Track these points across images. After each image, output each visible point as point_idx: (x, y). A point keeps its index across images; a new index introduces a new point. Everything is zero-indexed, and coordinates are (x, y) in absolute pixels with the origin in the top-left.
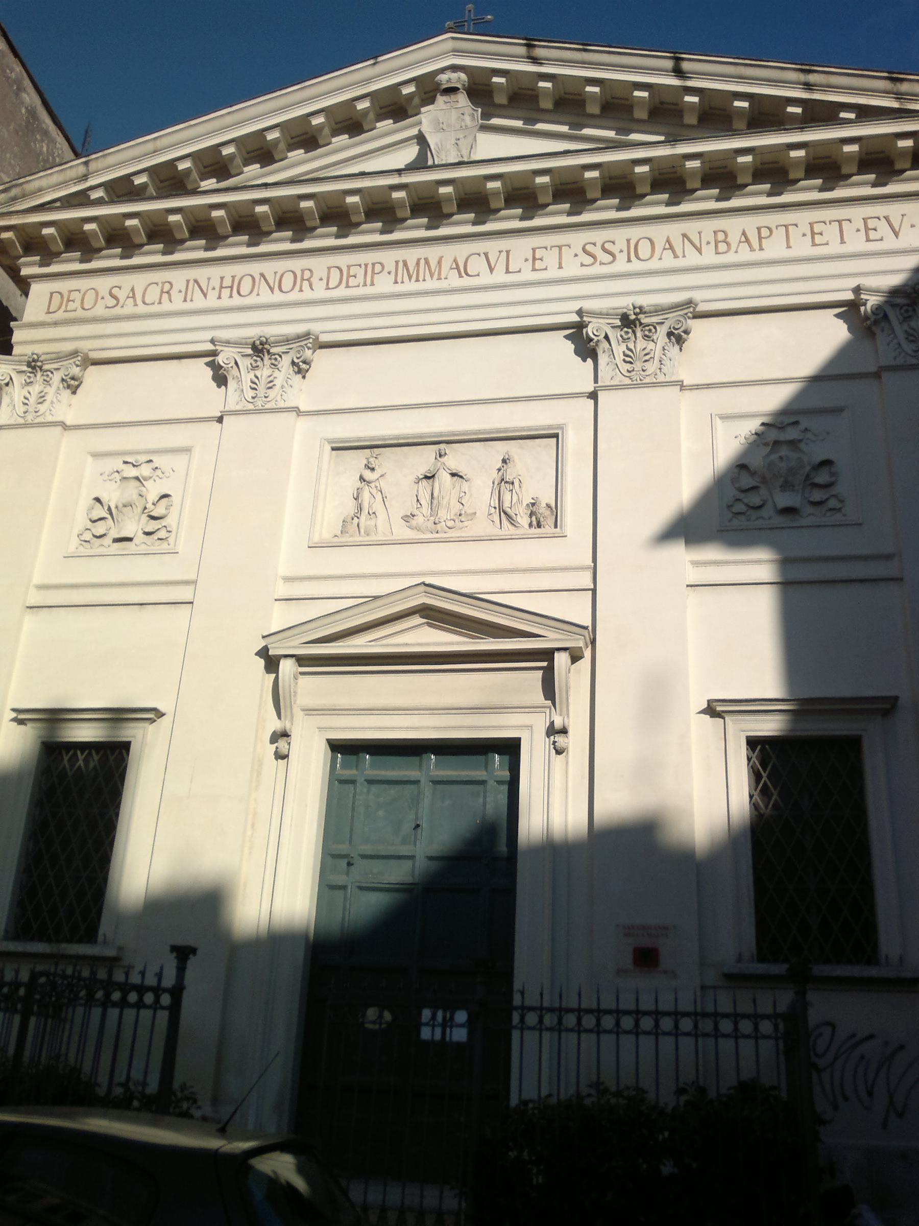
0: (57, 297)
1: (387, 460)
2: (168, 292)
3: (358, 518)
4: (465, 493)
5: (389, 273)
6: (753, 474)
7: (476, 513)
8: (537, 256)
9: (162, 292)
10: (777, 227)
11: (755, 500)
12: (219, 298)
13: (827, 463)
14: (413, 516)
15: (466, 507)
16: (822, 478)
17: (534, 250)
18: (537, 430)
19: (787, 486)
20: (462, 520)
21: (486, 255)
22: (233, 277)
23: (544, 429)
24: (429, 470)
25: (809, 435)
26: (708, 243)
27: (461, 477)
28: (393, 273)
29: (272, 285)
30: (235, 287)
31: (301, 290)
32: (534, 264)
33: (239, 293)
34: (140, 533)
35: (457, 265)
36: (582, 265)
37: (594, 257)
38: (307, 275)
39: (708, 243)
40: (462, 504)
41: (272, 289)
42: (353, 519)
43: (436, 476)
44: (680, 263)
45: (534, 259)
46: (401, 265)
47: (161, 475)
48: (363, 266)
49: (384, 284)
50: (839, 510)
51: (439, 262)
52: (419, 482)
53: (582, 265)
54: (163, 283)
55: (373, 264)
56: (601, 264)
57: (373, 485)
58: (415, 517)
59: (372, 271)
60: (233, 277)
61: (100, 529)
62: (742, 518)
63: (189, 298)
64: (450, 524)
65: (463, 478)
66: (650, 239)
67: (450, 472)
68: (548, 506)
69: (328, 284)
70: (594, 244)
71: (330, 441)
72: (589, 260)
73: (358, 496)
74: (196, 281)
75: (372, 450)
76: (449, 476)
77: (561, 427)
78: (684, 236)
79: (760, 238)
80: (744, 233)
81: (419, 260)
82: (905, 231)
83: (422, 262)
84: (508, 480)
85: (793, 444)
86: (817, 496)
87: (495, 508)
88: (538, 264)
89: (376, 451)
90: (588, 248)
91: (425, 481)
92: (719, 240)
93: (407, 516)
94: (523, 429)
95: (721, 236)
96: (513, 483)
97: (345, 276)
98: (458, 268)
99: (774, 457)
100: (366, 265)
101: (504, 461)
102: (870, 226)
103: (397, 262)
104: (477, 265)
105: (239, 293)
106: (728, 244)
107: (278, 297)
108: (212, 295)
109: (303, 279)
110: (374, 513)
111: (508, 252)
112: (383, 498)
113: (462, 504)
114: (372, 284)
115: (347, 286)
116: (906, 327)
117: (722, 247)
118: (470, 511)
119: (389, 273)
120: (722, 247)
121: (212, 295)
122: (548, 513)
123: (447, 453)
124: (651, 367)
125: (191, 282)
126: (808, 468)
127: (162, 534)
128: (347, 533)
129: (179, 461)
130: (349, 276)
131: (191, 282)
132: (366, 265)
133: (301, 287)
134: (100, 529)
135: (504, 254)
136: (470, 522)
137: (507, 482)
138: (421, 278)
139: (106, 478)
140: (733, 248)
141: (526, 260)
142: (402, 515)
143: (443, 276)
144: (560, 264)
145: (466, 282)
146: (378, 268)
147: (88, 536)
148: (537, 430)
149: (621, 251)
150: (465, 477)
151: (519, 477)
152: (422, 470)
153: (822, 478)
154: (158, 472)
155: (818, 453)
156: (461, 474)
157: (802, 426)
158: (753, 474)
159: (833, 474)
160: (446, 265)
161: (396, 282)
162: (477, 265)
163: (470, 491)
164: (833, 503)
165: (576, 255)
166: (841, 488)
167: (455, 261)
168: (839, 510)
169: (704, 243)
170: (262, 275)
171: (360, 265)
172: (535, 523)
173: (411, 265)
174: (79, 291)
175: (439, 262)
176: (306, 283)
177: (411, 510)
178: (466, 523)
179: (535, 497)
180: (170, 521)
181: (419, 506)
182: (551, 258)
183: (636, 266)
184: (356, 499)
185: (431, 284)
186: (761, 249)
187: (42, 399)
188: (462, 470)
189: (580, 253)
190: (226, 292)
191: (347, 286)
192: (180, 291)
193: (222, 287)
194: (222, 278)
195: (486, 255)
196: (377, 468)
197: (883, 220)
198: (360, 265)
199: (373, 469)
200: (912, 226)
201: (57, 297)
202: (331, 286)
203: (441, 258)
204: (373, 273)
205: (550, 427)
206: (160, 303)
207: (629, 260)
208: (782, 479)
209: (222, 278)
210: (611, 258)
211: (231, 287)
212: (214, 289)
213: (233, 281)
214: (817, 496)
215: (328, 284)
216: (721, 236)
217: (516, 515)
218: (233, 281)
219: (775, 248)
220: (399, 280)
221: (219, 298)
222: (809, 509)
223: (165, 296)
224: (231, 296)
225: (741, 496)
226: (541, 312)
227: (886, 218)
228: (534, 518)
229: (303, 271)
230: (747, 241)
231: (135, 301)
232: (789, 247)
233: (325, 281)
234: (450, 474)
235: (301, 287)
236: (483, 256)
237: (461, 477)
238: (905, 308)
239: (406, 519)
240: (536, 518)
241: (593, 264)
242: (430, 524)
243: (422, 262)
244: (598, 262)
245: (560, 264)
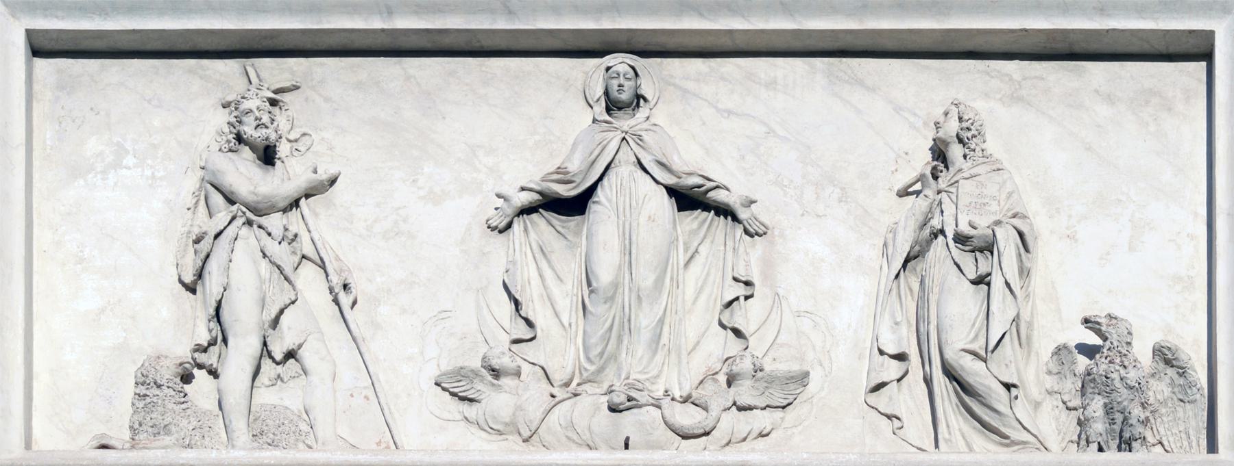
3: (214, 373)
4: (748, 284)
7: (806, 374)
14: (496, 373)
15: (757, 345)
20: (744, 400)
24: (559, 171)
27: (725, 211)
40: (737, 333)
42: (187, 378)
52: (509, 226)
58: (505, 381)
64: (688, 417)
65: (735, 219)
67: (670, 180)
68: (1166, 357)
73: (200, 275)
75: (249, 62)
76: (666, 204)
84: (964, 228)
87: (901, 357)
89: (274, 71)
93: (460, 373)
96: (988, 248)
101: (940, 154)
110: (290, 355)
112: (331, 290)
113: (737, 333)
122: (1159, 390)
123: (646, 90)
128: (168, 433)
136: (779, 414)
137: (961, 239)
142: (432, 372)
150: (743, 214)
151: (1016, 222)
156: (719, 196)
163: (767, 276)
172: (1098, 427)
177: (483, 349)
179: (1097, 311)
181: (523, 332)
184: (192, 289)
196: (283, 149)
199: (268, 156)
217: (1008, 386)
228: (1097, 406)
234: (672, 191)
237: (725, 211)
239: (462, 388)
240: (1109, 410)
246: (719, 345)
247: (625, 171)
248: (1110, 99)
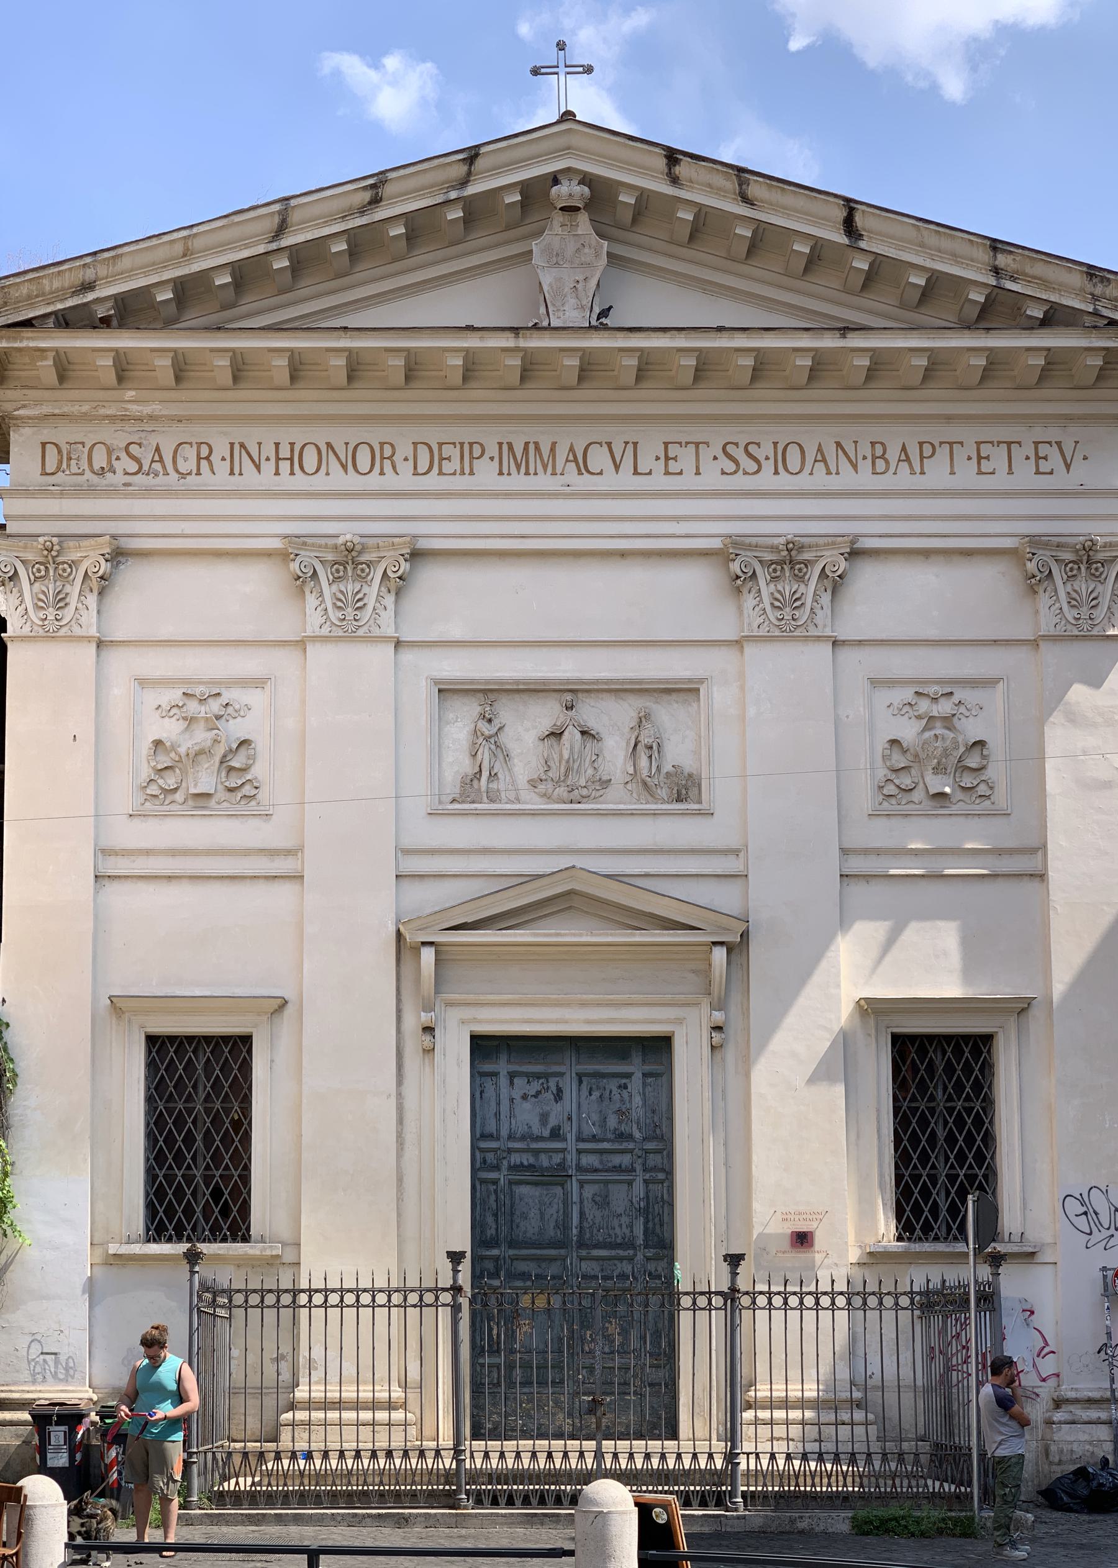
0: (51, 451)
1: (507, 712)
2: (207, 458)
5: (492, 459)
6: (905, 751)
8: (671, 455)
9: (199, 458)
10: (941, 443)
11: (906, 781)
12: (277, 473)
13: (980, 744)
16: (973, 761)
17: (666, 444)
18: (676, 683)
19: (938, 770)
21: (609, 444)
22: (292, 444)
23: (684, 683)
24: (555, 725)
25: (962, 709)
26: (865, 458)
27: (594, 736)
28: (497, 459)
29: (344, 462)
30: (296, 460)
31: (382, 473)
32: (666, 465)
33: (302, 468)
34: (220, 787)
35: (575, 456)
36: (723, 473)
37: (736, 462)
38: (388, 452)
39: (865, 458)
41: (344, 467)
43: (566, 733)
44: (833, 483)
45: (667, 458)
46: (505, 447)
47: (235, 714)
48: (458, 446)
49: (486, 474)
50: (988, 797)
51: (553, 449)
53: (723, 473)
54: (199, 444)
55: (471, 444)
56: (746, 473)
57: (492, 741)
59: (471, 453)
60: (292, 444)
61: (170, 781)
62: (893, 801)
63: (237, 471)
64: (585, 792)
66: (799, 445)
69: (415, 468)
70: (736, 444)
71: (436, 682)
72: (731, 467)
74: (242, 445)
76: (579, 734)
77: (701, 681)
78: (838, 444)
79: (922, 458)
80: (904, 449)
81: (527, 444)
82: (1077, 465)
83: (532, 447)
85: (948, 721)
86: (968, 780)
88: (673, 466)
90: (730, 449)
91: (553, 739)
92: (877, 455)
94: (660, 681)
95: (879, 451)
97: (437, 461)
98: (576, 460)
99: (927, 735)
100: (462, 444)
102: (1041, 455)
103: (500, 444)
104: (599, 459)
105: (302, 468)
106: (887, 462)
107: (352, 481)
108: (268, 467)
109: (382, 458)
111: (635, 444)
114: (472, 473)
115: (441, 473)
116: (1069, 588)
117: (880, 465)
118: (605, 778)
119: (492, 459)
120: (880, 465)
121: (268, 467)
124: (803, 615)
125: (237, 447)
126: (962, 749)
127: (247, 790)
129: (254, 698)
130: (441, 459)
131: (237, 447)
132: (462, 444)
133: (382, 469)
134: (170, 781)
135: (630, 447)
138: (532, 471)
139: (164, 714)
140: (892, 469)
141: (658, 458)
143: (559, 471)
144: (698, 468)
145: (585, 482)
146: (477, 451)
147: (153, 790)
148: (676, 683)
149: (767, 458)
152: (546, 726)
153: (973, 761)
154: (230, 710)
155: (972, 729)
156: (592, 732)
157: (956, 698)
158: (905, 751)
159: (984, 757)
160: (562, 454)
161: (501, 473)
162: (599, 459)
164: (982, 789)
165: (715, 458)
166: (990, 773)
167: (572, 449)
168: (988, 797)
169: (860, 458)
170: (329, 445)
171: (454, 444)
173: (519, 450)
174: (83, 444)
175: (553, 449)
176: (387, 463)
178: (601, 793)
180: (258, 771)
182: (686, 459)
183: (783, 481)
185: (543, 481)
186: (922, 473)
187: (61, 601)
188: (593, 724)
189: (720, 455)
190: (285, 466)
191: (441, 473)
192: (223, 459)
193: (278, 459)
194: (277, 445)
195: (609, 444)
197: (1054, 445)
198: (454, 444)
199: (490, 721)
200: (1085, 458)
201: (51, 451)
202: (420, 471)
203: (554, 444)
204: (472, 458)
205: (690, 681)
206: (198, 473)
207: (776, 473)
208: (936, 761)
209: (277, 445)
210: (755, 467)
211: (291, 459)
212: (268, 459)
213: (292, 450)
214: (968, 780)
215: (415, 468)
216: (879, 451)
218: (292, 450)
219: (937, 474)
220: (505, 471)
221: (277, 473)
222: (960, 795)
223: (204, 463)
224: (292, 473)
225: (893, 776)
226: (678, 532)
227: (1059, 444)
229: (382, 444)
230: (908, 460)
231: (164, 467)
232: (952, 473)
233: (411, 462)
235: (382, 469)
236: (605, 447)
238: (1070, 565)
241: (735, 472)
242: (561, 791)
243: (532, 447)
244: (741, 472)
245: (698, 468)
246: (590, 772)
247: (571, 727)
248: (677, 702)
